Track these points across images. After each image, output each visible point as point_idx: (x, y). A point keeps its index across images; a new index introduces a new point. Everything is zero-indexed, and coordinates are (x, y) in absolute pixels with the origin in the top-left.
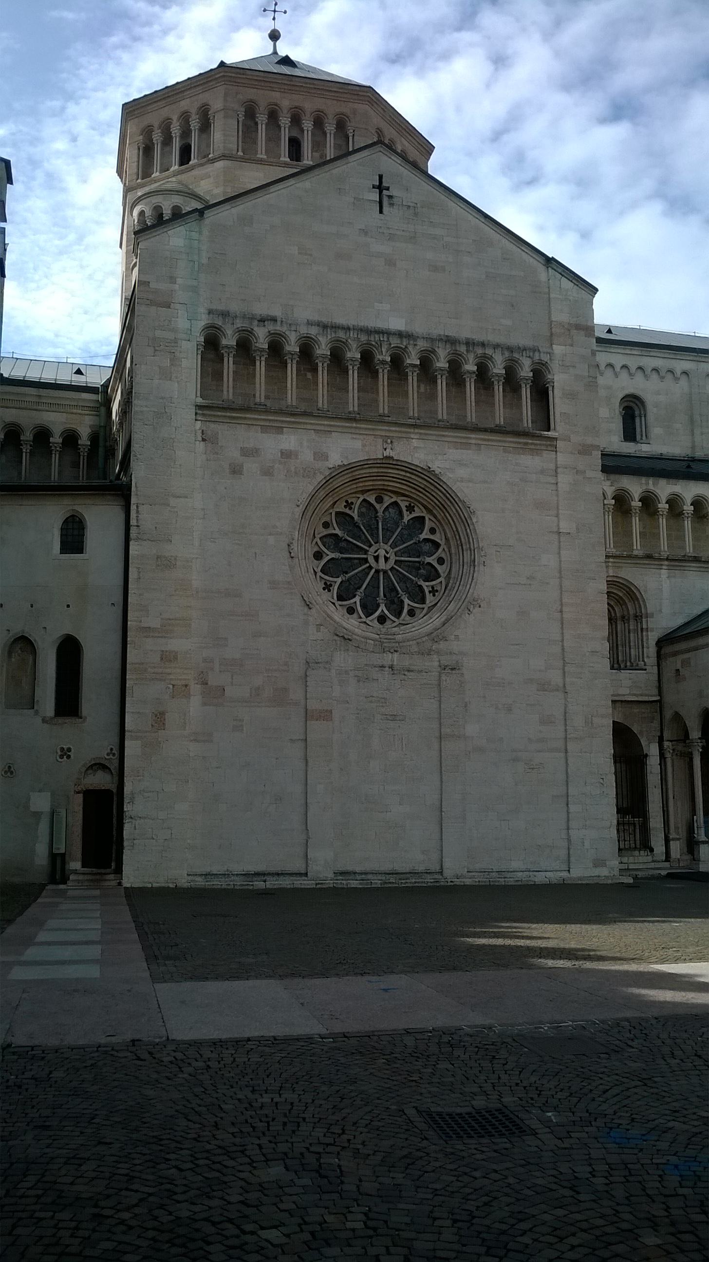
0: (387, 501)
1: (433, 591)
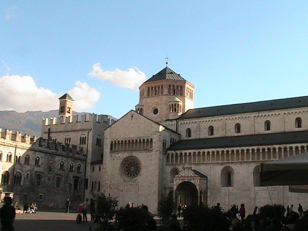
0: (134, 160)
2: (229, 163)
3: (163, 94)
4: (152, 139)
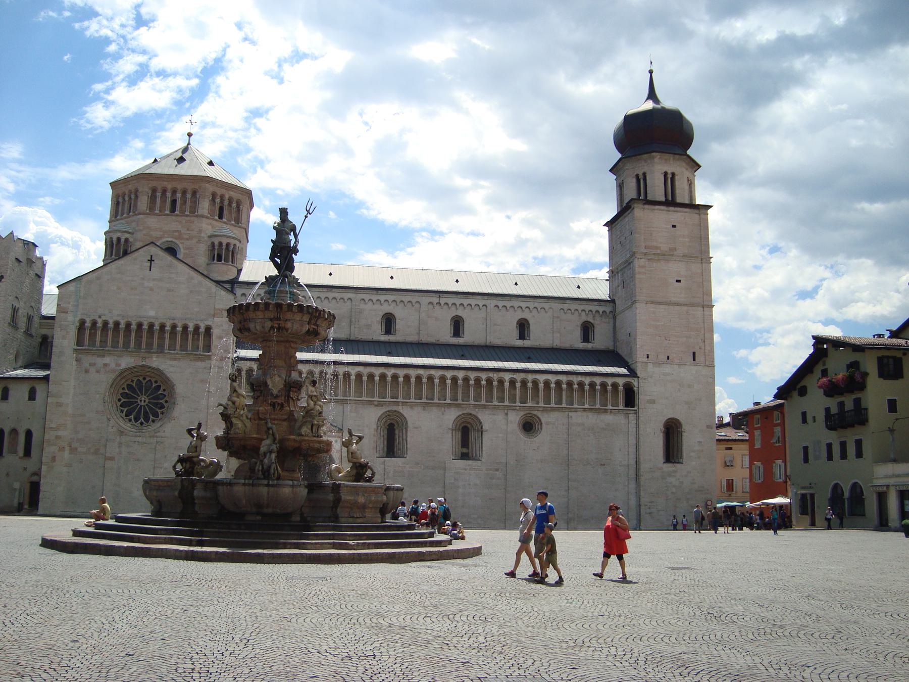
0: (148, 379)
1: (162, 413)
2: (397, 403)
3: (196, 213)
4: (208, 329)
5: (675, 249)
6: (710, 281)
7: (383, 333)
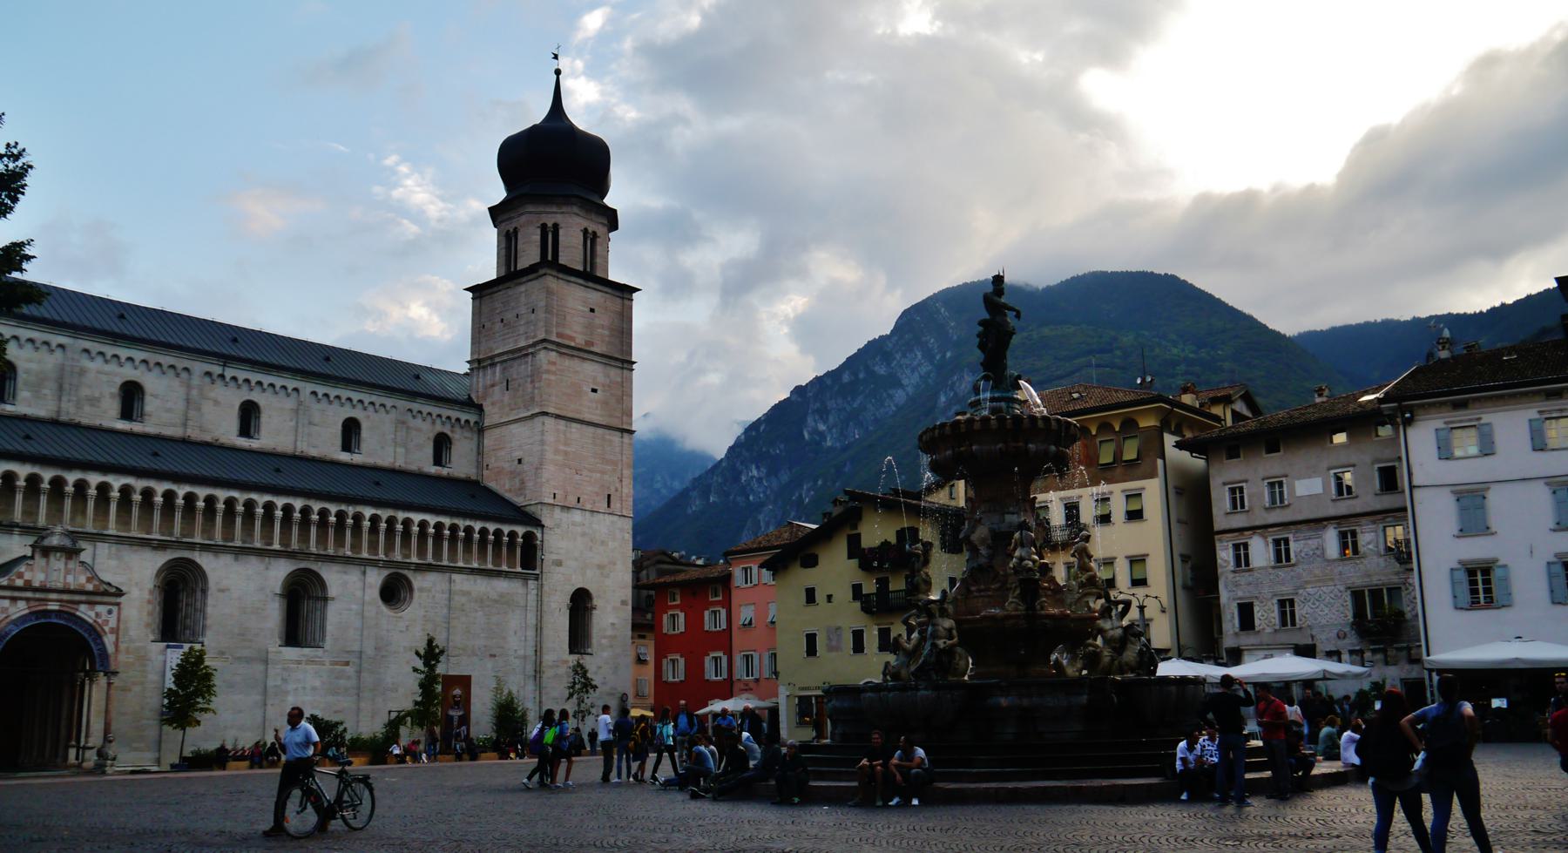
2: (192, 546)
5: (592, 344)
6: (631, 396)
7: (119, 417)
